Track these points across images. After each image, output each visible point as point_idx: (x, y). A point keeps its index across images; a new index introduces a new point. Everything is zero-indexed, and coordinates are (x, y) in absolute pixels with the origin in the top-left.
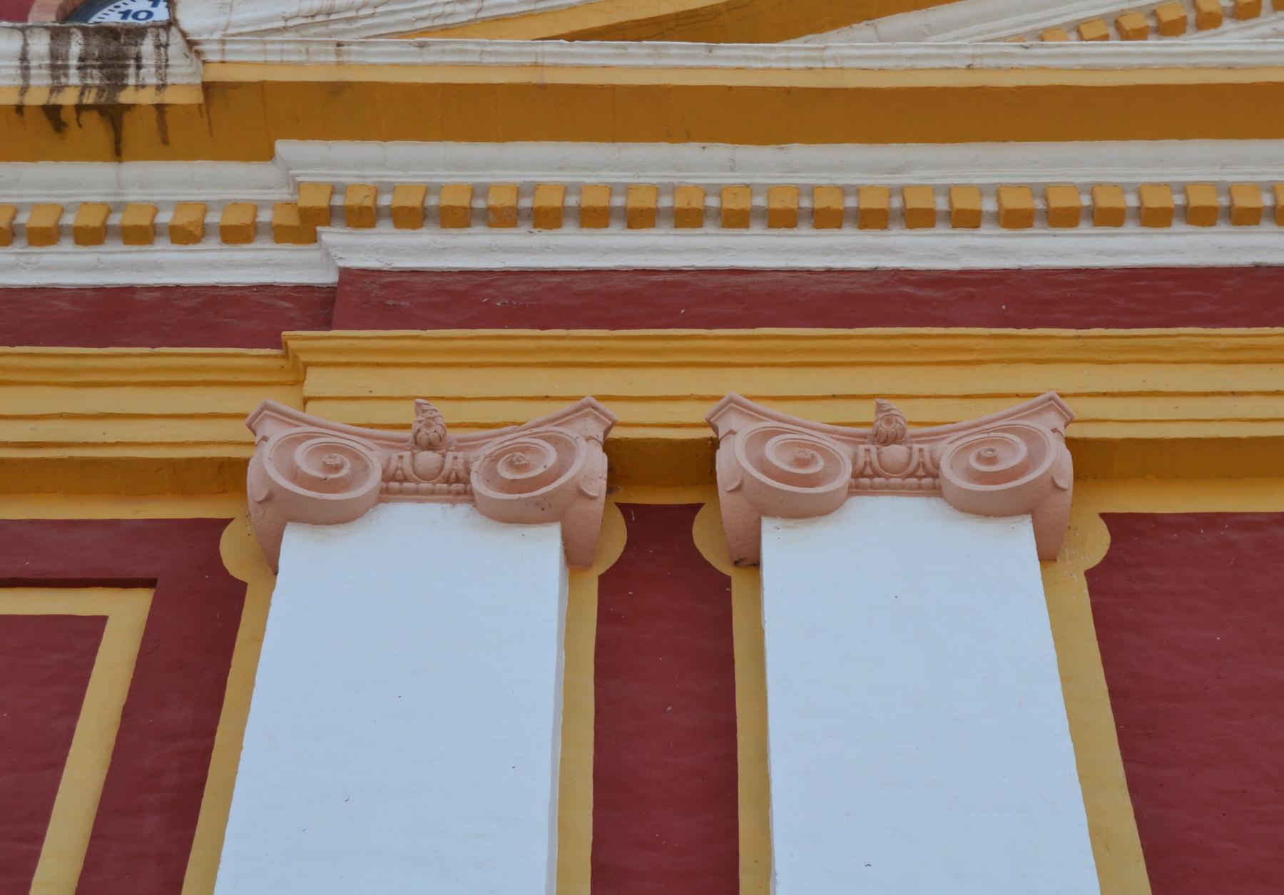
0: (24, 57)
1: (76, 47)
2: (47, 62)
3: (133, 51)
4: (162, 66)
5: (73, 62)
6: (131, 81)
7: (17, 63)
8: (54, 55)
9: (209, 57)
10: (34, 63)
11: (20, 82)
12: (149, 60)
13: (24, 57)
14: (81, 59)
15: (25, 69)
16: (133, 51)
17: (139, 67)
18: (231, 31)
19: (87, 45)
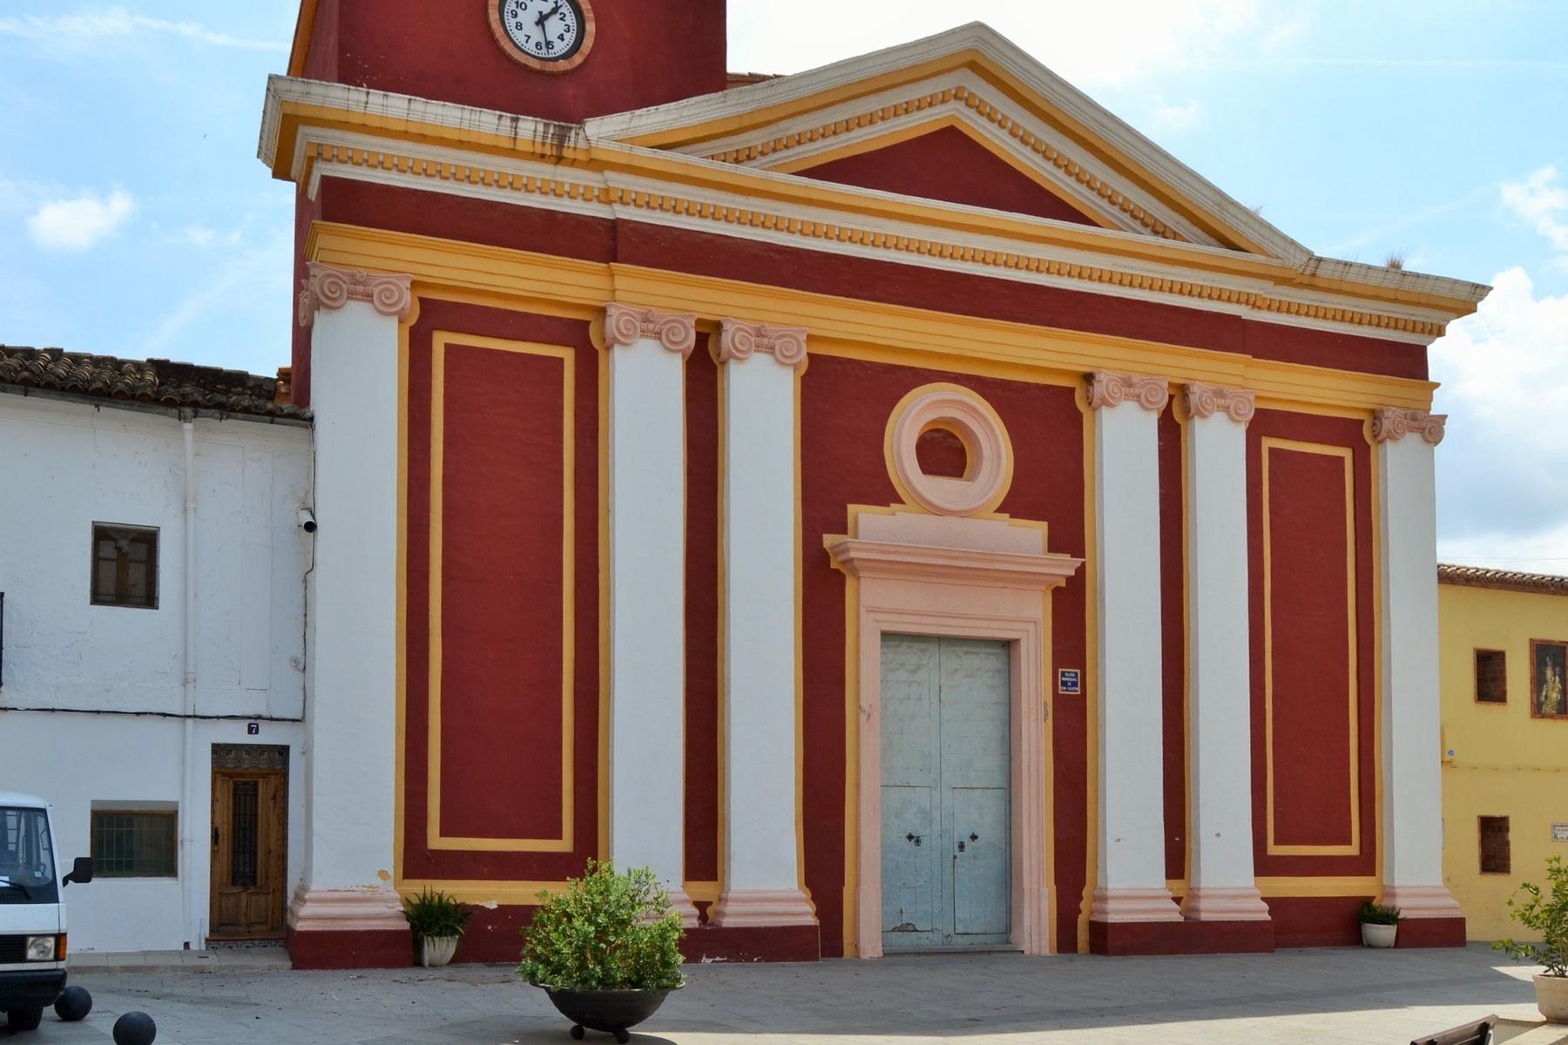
0: (535, 131)
1: (551, 131)
2: (542, 134)
3: (568, 134)
4: (576, 142)
5: (550, 136)
6: (566, 145)
7: (532, 133)
8: (544, 133)
9: (592, 145)
10: (538, 134)
11: (532, 139)
12: (572, 139)
13: (535, 131)
14: (553, 135)
15: (535, 136)
16: (568, 134)
17: (569, 140)
18: (600, 136)
19: (555, 130)
